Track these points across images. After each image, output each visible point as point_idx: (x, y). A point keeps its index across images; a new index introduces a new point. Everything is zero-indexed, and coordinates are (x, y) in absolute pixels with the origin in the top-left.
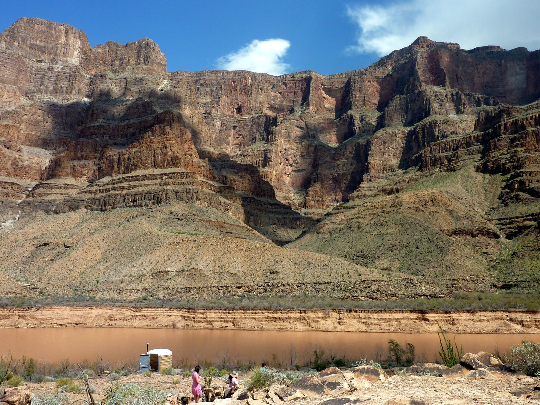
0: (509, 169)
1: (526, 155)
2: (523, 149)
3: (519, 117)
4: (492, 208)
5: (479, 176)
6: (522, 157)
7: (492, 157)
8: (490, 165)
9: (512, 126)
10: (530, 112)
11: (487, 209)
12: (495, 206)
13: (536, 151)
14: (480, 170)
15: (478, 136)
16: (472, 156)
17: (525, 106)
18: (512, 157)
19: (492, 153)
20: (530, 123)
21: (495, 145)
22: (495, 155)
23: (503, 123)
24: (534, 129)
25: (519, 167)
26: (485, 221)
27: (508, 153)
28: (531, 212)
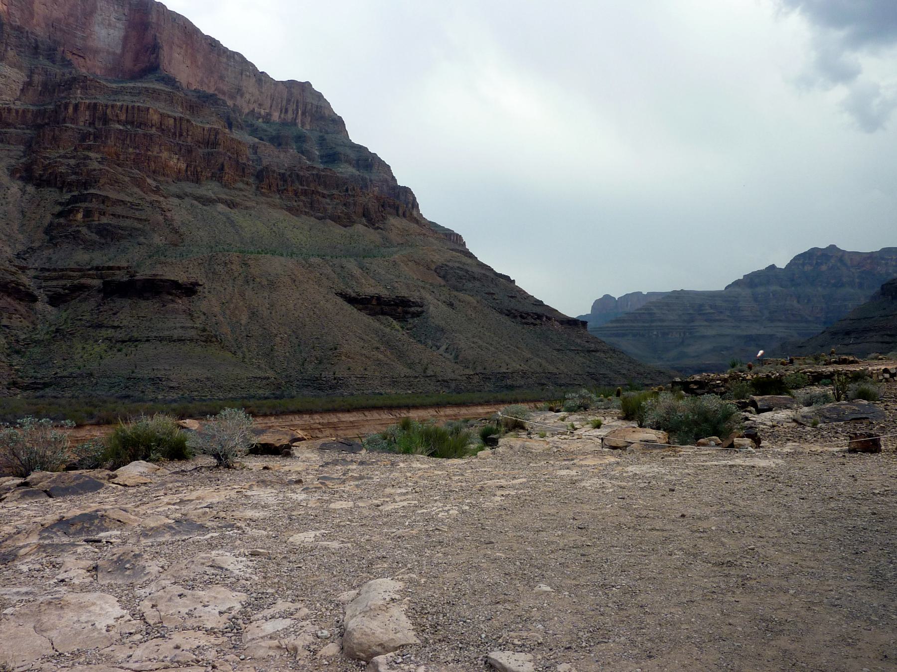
0: (70, 184)
1: (101, 167)
2: (98, 156)
3: (101, 100)
4: (31, 248)
5: (15, 188)
6: (95, 170)
7: (45, 158)
8: (38, 172)
9: (87, 113)
10: (120, 97)
11: (20, 247)
12: (36, 245)
13: (118, 165)
14: (18, 175)
15: (24, 111)
16: (8, 147)
17: (114, 85)
18: (78, 165)
19: (45, 148)
20: (117, 116)
21: (53, 137)
22: (53, 154)
23: (74, 102)
24: (121, 127)
25: (86, 185)
26: (13, 269)
27: (74, 157)
28: (95, 263)
